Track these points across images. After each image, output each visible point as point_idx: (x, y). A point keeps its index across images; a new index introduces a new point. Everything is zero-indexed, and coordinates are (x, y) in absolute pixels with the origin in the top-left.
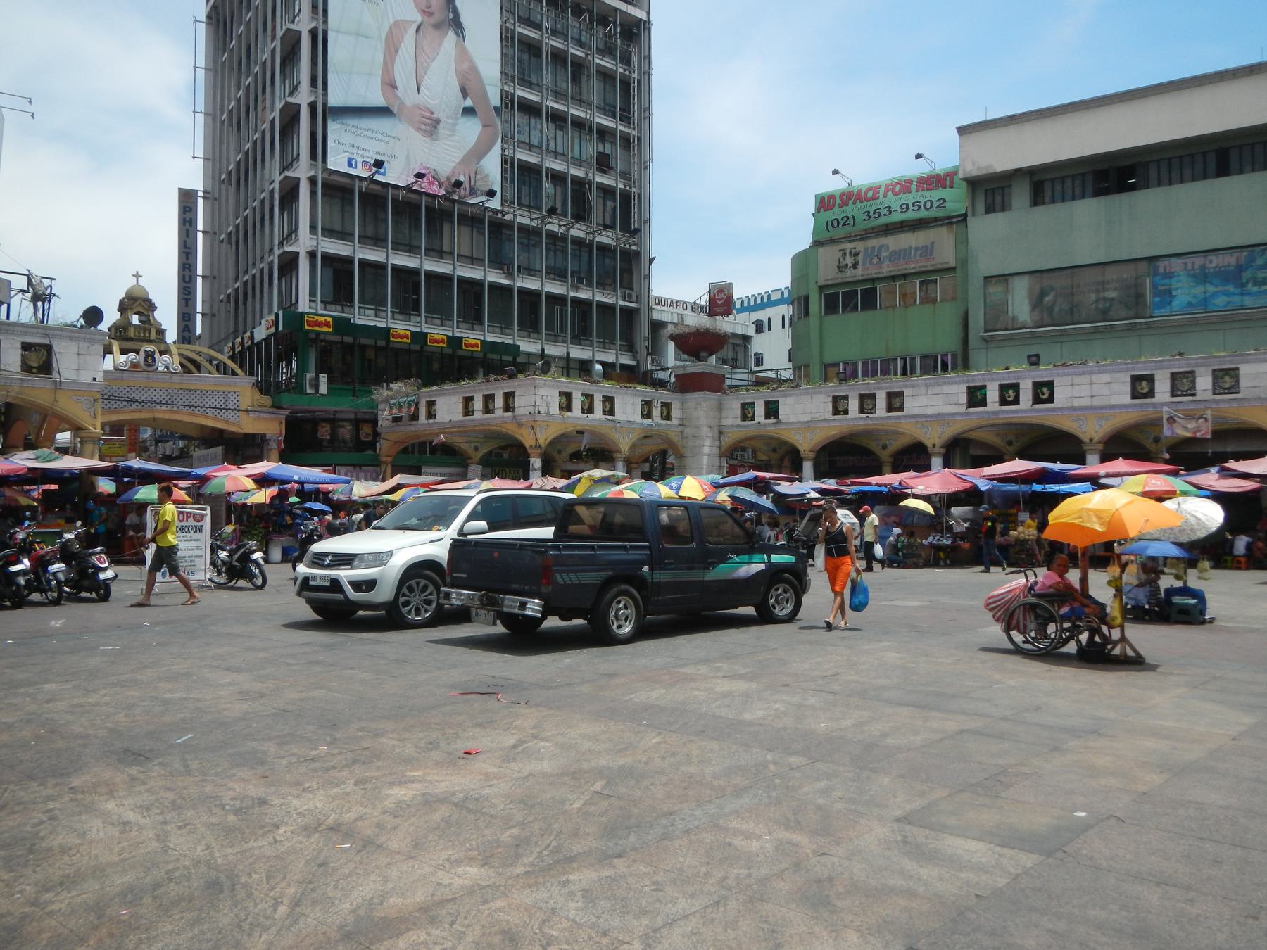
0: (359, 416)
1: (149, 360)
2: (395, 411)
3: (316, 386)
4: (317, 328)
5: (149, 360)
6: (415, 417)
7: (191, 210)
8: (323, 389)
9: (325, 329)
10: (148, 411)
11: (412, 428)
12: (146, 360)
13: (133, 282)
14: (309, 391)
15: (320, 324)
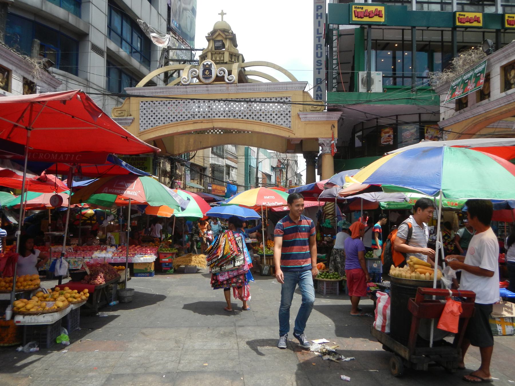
0: (424, 118)
1: (207, 73)
2: (459, 93)
3: (369, 82)
4: (366, 19)
5: (207, 73)
6: (484, 94)
7: (321, 7)
8: (377, 87)
9: (376, 19)
10: (208, 122)
11: (481, 110)
12: (204, 74)
13: (219, 19)
14: (362, 89)
15: (369, 15)
